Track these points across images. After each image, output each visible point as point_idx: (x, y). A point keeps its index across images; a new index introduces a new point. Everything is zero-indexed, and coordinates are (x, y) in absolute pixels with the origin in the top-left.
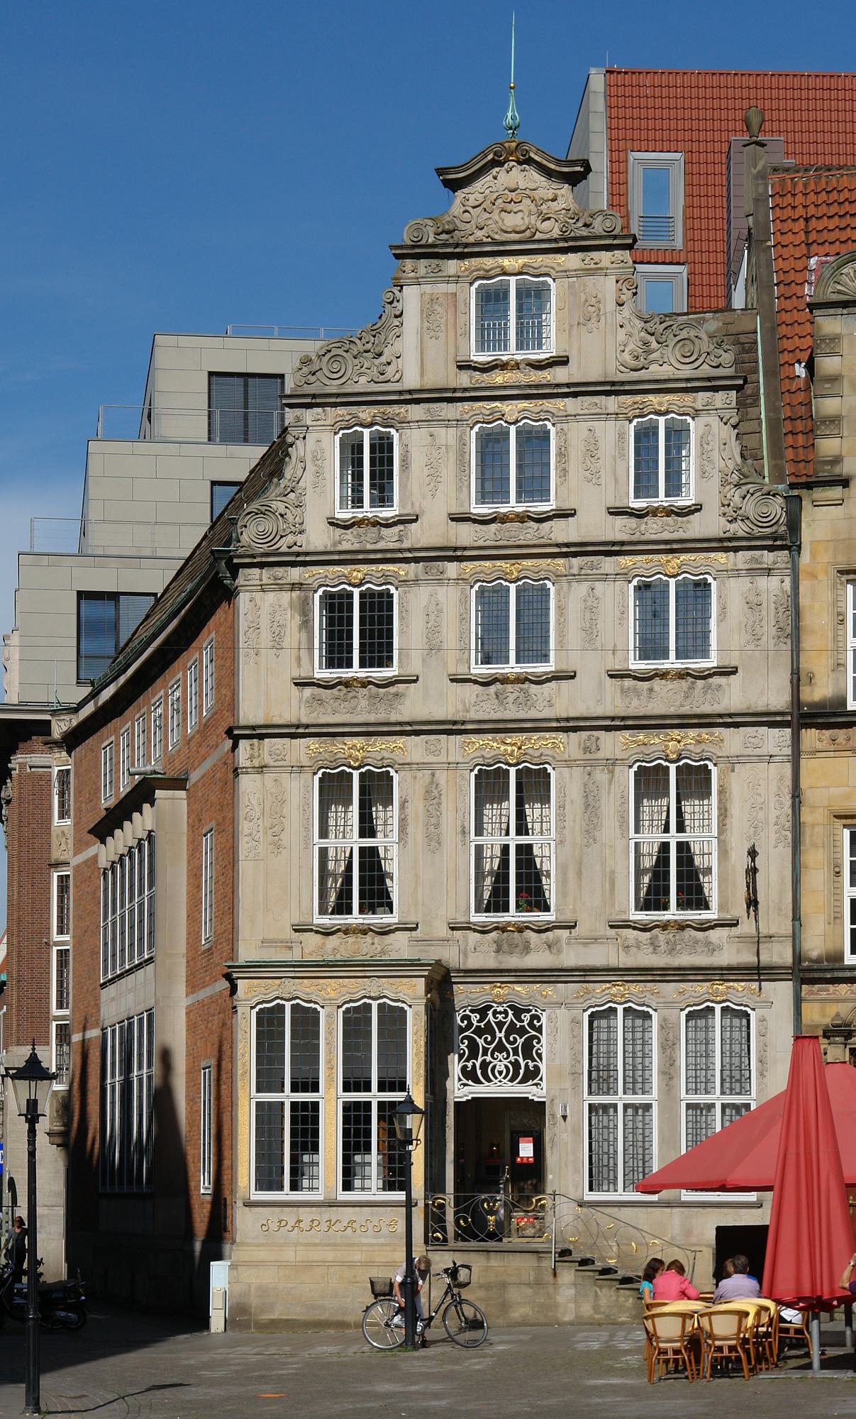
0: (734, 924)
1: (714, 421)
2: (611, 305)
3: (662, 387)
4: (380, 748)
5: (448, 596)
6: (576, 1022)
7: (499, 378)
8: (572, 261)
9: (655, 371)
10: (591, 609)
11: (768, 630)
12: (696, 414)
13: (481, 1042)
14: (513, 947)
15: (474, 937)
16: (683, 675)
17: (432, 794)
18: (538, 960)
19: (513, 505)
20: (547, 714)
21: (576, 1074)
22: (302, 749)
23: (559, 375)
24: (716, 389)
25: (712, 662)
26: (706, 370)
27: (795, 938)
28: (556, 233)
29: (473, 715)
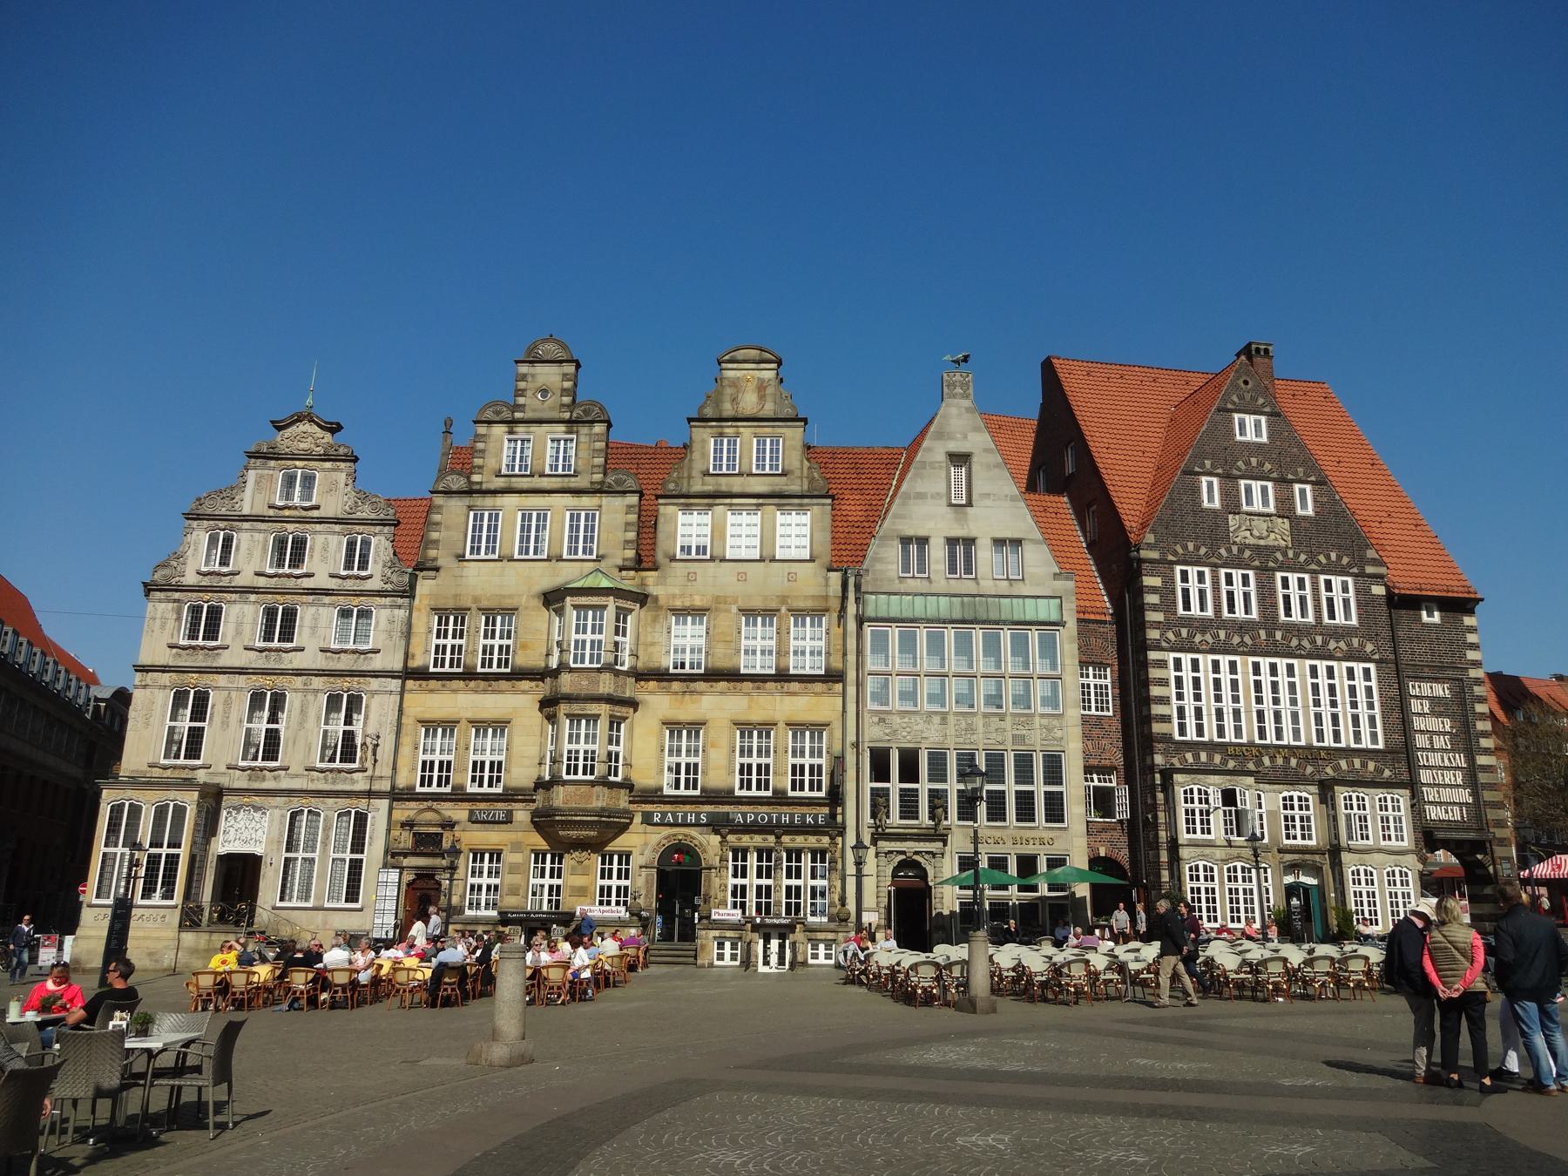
1: (383, 538)
2: (342, 485)
4: (207, 680)
6: (283, 816)
7: (287, 513)
8: (328, 465)
10: (316, 619)
12: (375, 535)
14: (257, 779)
16: (354, 652)
17: (228, 703)
18: (269, 784)
20: (290, 666)
22: (166, 678)
23: (315, 513)
24: (385, 525)
25: (370, 647)
26: (382, 516)
27: (393, 778)
28: (322, 452)
29: (253, 666)
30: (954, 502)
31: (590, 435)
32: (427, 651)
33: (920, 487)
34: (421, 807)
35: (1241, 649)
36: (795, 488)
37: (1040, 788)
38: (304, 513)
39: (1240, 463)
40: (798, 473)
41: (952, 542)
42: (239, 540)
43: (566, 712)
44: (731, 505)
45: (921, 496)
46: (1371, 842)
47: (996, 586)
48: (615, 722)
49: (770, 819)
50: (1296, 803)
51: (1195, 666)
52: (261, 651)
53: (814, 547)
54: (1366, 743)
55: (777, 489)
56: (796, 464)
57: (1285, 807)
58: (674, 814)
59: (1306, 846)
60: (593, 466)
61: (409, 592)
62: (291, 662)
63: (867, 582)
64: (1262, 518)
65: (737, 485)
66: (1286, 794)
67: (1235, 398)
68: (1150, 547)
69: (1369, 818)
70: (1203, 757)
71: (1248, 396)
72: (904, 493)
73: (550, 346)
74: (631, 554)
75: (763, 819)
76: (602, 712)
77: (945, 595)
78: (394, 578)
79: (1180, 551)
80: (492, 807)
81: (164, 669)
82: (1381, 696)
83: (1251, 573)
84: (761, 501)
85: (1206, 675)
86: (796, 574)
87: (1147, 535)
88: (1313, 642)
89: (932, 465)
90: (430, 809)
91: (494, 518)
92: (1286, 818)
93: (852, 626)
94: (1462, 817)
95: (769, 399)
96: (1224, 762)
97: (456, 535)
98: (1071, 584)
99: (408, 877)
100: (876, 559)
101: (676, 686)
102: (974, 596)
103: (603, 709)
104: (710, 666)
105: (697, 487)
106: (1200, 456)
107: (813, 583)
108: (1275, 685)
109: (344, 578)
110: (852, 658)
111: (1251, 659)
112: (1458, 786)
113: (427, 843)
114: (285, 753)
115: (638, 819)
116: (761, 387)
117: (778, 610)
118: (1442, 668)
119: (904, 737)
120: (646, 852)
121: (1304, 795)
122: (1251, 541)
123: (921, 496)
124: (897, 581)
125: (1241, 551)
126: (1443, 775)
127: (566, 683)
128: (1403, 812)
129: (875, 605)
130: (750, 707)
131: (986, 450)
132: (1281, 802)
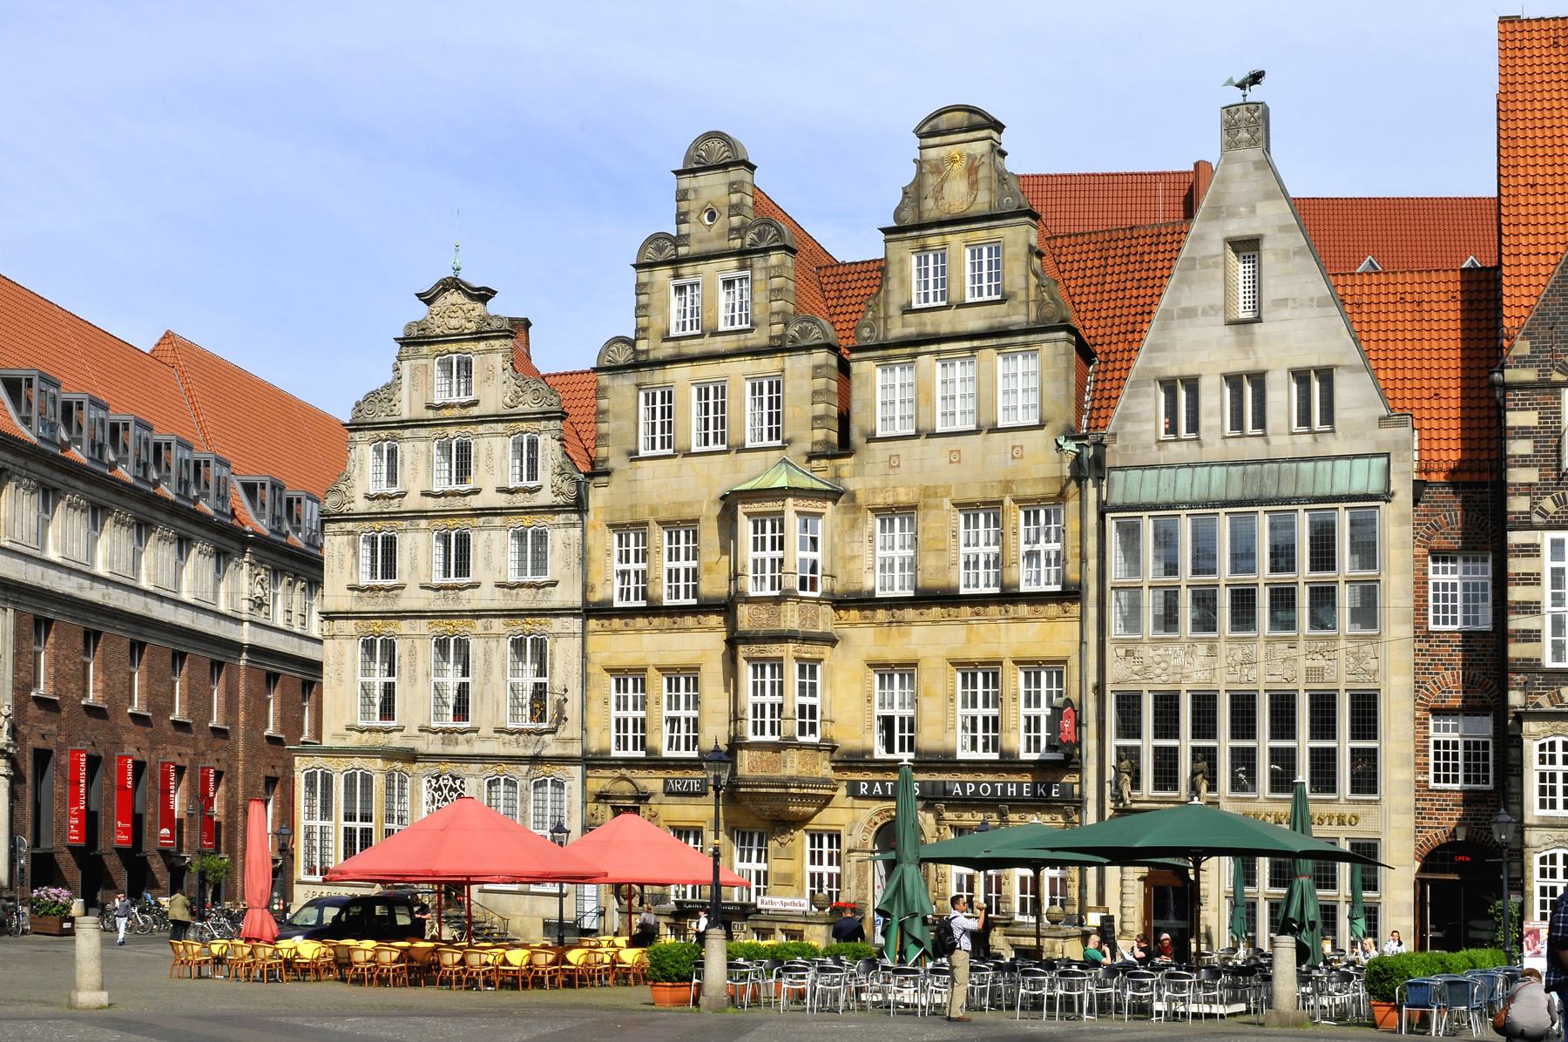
1: (548, 436)
5: (421, 538)
7: (446, 413)
8: (482, 345)
9: (522, 408)
10: (489, 547)
13: (436, 795)
16: (530, 586)
18: (462, 749)
23: (475, 411)
26: (546, 408)
28: (474, 329)
34: (616, 775)
38: (464, 412)
40: (1022, 296)
41: (1234, 381)
43: (745, 655)
44: (938, 352)
45: (1188, 313)
47: (1294, 444)
48: (808, 667)
49: (994, 789)
52: (438, 590)
53: (1045, 406)
55: (996, 322)
56: (1021, 282)
58: (882, 783)
60: (772, 314)
61: (579, 506)
63: (1113, 451)
65: (945, 322)
68: (1523, 362)
72: (1164, 311)
73: (716, 145)
75: (985, 788)
76: (784, 654)
80: (687, 776)
84: (976, 343)
86: (1022, 447)
87: (1518, 343)
90: (623, 778)
95: (982, 185)
97: (628, 425)
98: (1404, 432)
100: (1125, 418)
101: (881, 614)
104: (919, 585)
105: (897, 330)
110: (1093, 563)
115: (842, 791)
116: (972, 170)
117: (1001, 502)
123: (1188, 313)
124: (1155, 448)
127: (746, 617)
129: (1124, 486)
130: (968, 640)
131: (1284, 229)
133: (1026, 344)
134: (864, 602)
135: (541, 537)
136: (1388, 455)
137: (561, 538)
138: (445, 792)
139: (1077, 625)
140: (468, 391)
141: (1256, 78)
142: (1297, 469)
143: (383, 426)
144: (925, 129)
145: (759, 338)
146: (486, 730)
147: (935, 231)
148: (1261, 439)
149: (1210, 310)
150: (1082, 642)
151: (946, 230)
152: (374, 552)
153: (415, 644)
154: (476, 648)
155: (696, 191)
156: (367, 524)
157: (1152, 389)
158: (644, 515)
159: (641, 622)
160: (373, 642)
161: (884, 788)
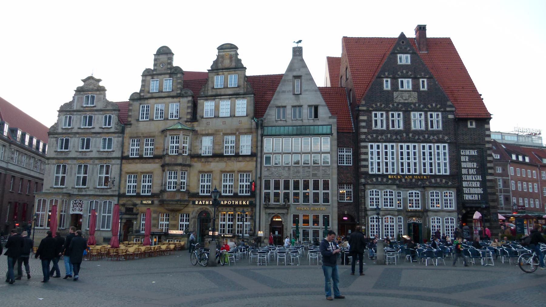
0: (111, 188)
1: (114, 115)
2: (102, 99)
3: (108, 110)
4: (66, 161)
5: (76, 139)
7: (87, 109)
8: (98, 93)
9: (108, 108)
11: (119, 146)
13: (75, 205)
15: (75, 190)
16: (107, 152)
17: (71, 168)
18: (84, 193)
19: (87, 127)
21: (87, 210)
22: (54, 161)
23: (95, 108)
26: (114, 108)
30: (296, 93)
31: (177, 78)
32: (129, 151)
33: (284, 89)
34: (127, 199)
35: (396, 141)
36: (242, 91)
37: (321, 191)
39: (399, 73)
40: (243, 86)
42: (73, 118)
44: (221, 98)
46: (440, 208)
47: (309, 122)
49: (232, 203)
50: (414, 195)
51: (378, 147)
54: (442, 173)
55: (236, 92)
57: (410, 196)
59: (416, 210)
60: (178, 88)
61: (122, 132)
62: (89, 155)
64: (407, 92)
66: (410, 192)
67: (398, 49)
68: (363, 105)
69: (440, 200)
70: (380, 179)
71: (403, 48)
74: (189, 117)
76: (178, 169)
77: (291, 126)
78: (118, 127)
79: (374, 106)
81: (53, 158)
82: (449, 155)
83: (401, 113)
84: (230, 97)
85: (382, 150)
87: (362, 101)
88: (424, 137)
89: (288, 81)
91: (148, 107)
92: (410, 200)
93: (259, 138)
94: (478, 198)
96: (387, 181)
99: (124, 221)
100: (268, 115)
101: (203, 160)
102: (301, 126)
103: (179, 168)
105: (210, 93)
106: (383, 71)
107: (247, 123)
108: (408, 154)
109: (103, 128)
110: (259, 148)
111: (400, 144)
112: (477, 187)
113: (129, 211)
114: (88, 183)
115: (191, 203)
117: (236, 133)
118: (475, 144)
119: (276, 175)
120: (193, 214)
121: (417, 192)
122: (402, 101)
124: (275, 122)
125: (398, 105)
126: (472, 184)
127: (167, 160)
128: (453, 197)
130: (226, 166)
132: (408, 195)
133: (243, 98)
134: (199, 156)
135: (110, 140)
136: (331, 125)
137: (116, 140)
138: (78, 204)
139: (255, 163)
140: (93, 104)
141: (300, 41)
142: (310, 128)
143: (69, 111)
144: (220, 48)
145: (174, 94)
146: (91, 188)
147: (221, 71)
148: (301, 121)
149: (289, 91)
150: (256, 167)
151: (224, 70)
152: (62, 143)
153: (72, 167)
154: (90, 167)
155: (159, 59)
156: (61, 135)
157: (275, 109)
158: (140, 135)
159: (137, 161)
160: (60, 165)
161: (202, 202)
